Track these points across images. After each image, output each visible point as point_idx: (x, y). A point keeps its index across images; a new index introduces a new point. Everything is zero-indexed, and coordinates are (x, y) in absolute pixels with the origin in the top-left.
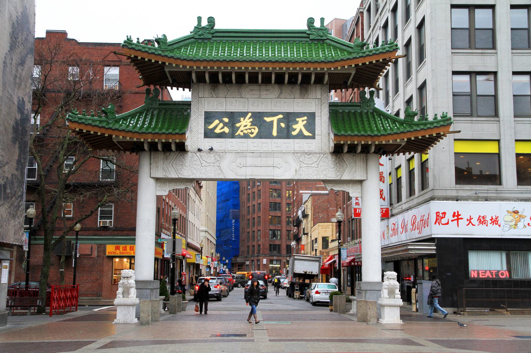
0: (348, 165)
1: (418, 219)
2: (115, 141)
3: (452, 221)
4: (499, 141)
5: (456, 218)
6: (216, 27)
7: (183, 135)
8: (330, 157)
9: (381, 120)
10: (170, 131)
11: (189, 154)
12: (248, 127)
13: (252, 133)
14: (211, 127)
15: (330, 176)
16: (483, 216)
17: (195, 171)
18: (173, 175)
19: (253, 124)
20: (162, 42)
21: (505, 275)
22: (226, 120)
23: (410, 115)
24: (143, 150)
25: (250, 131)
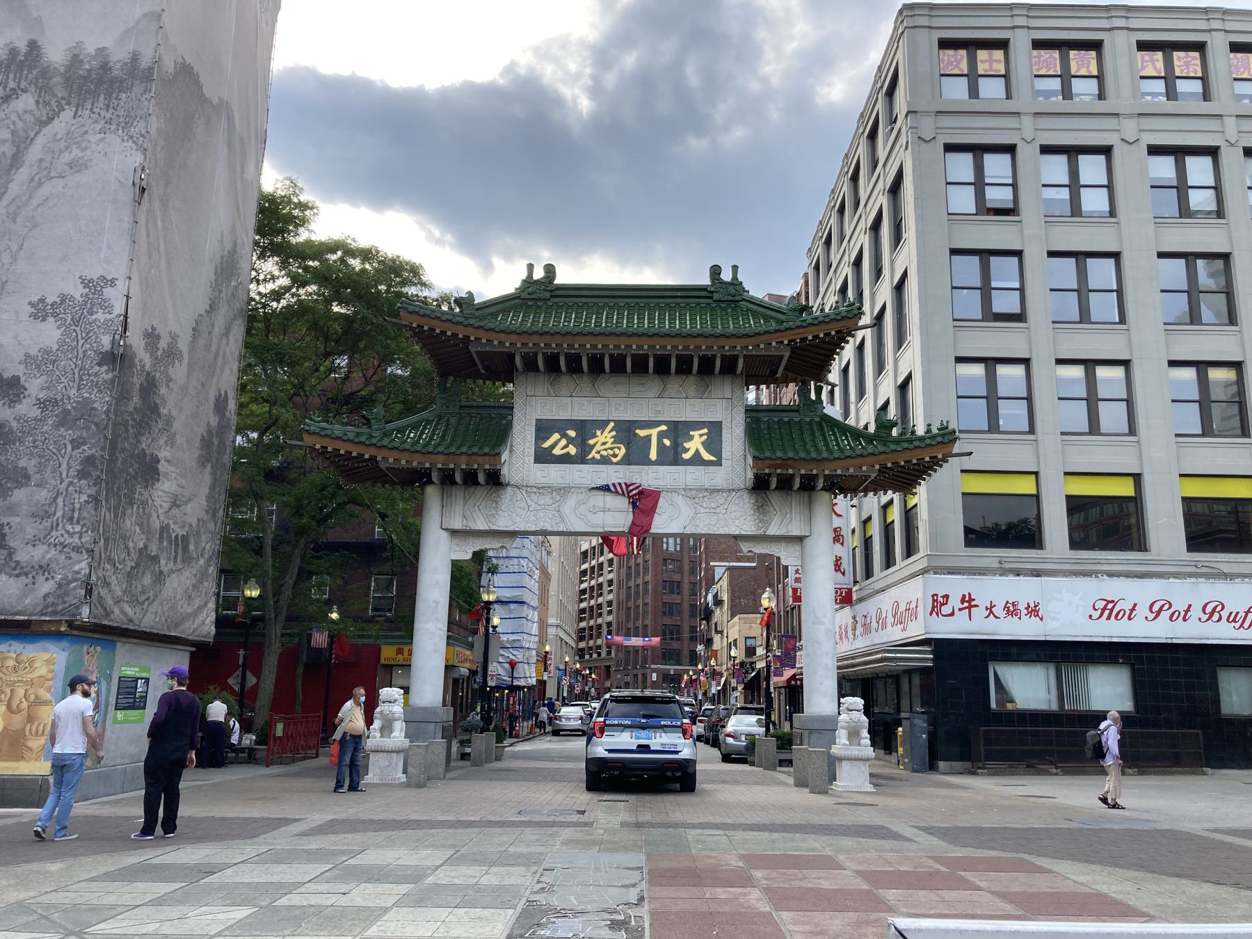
0: (778, 510)
1: (902, 608)
2: (383, 466)
3: (960, 610)
4: (1036, 474)
5: (966, 604)
6: (558, 281)
7: (497, 457)
8: (746, 496)
9: (834, 434)
10: (475, 450)
11: (509, 489)
12: (608, 445)
13: (615, 456)
14: (547, 445)
15: (748, 529)
16: (1013, 603)
17: (517, 519)
18: (481, 525)
19: (617, 440)
20: (466, 303)
21: (1054, 707)
22: (572, 433)
23: (884, 425)
24: (430, 482)
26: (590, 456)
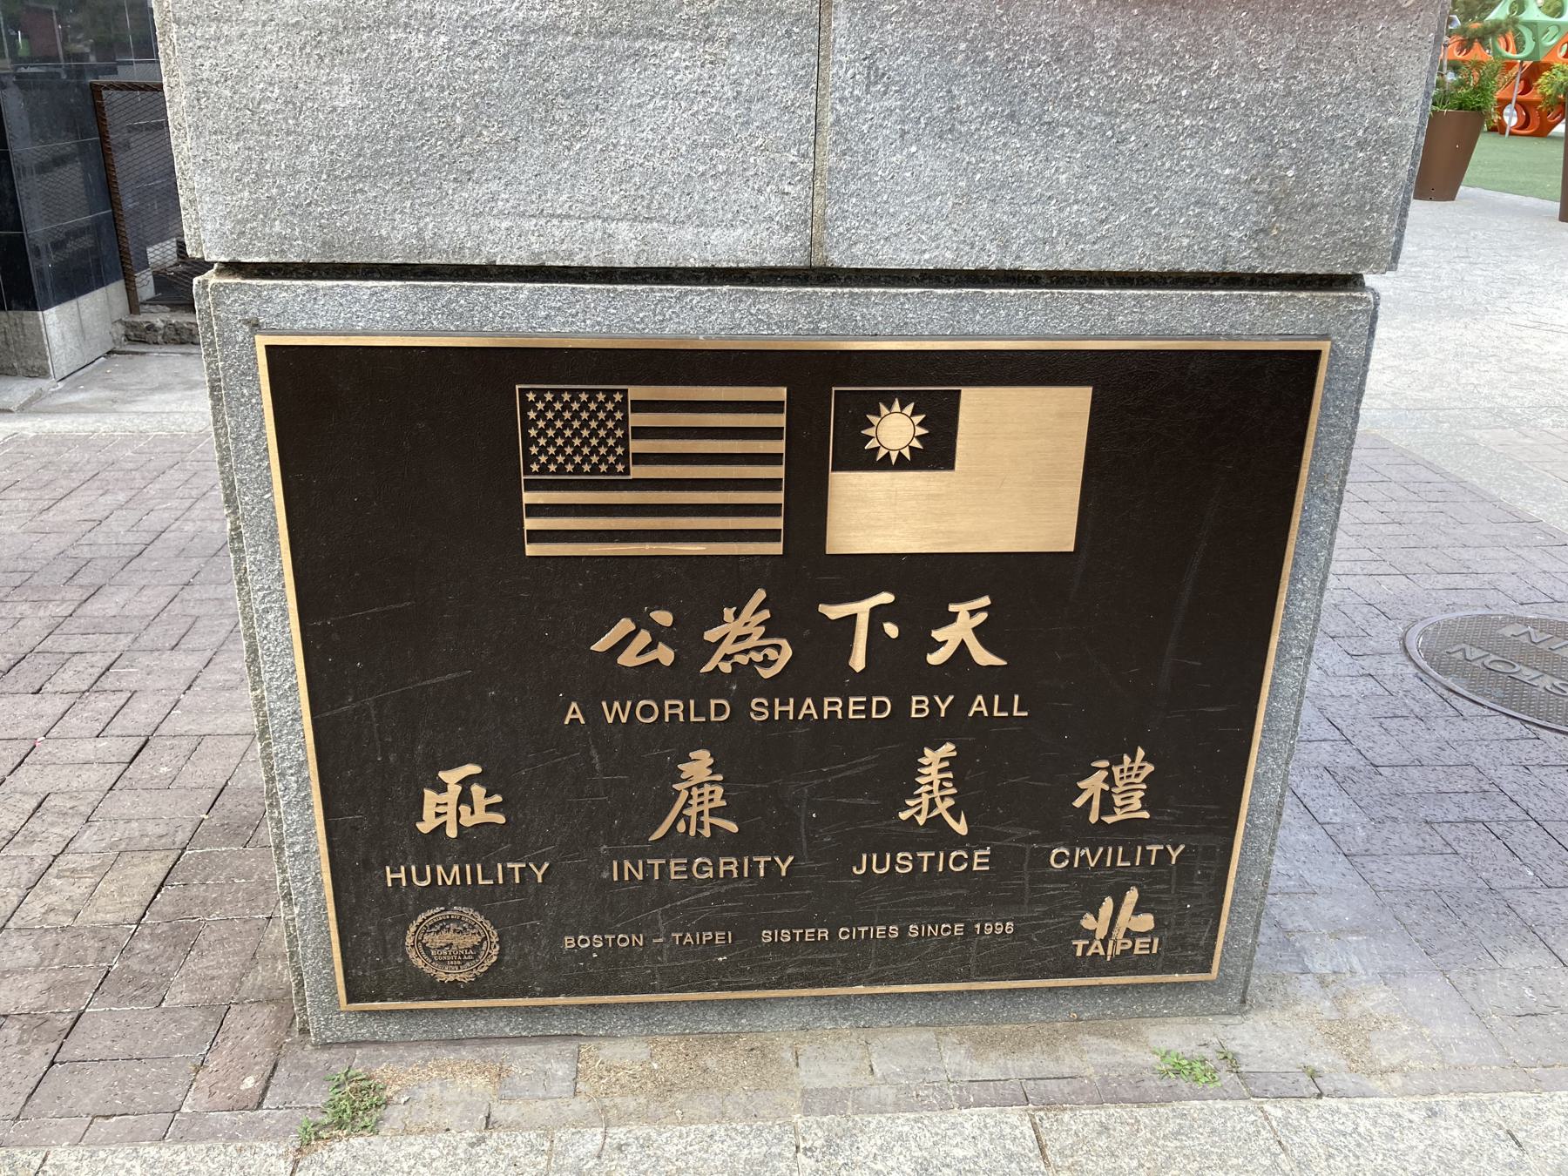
12: (753, 641)
13: (767, 663)
19: (771, 629)
25: (758, 657)
26: (708, 668)
